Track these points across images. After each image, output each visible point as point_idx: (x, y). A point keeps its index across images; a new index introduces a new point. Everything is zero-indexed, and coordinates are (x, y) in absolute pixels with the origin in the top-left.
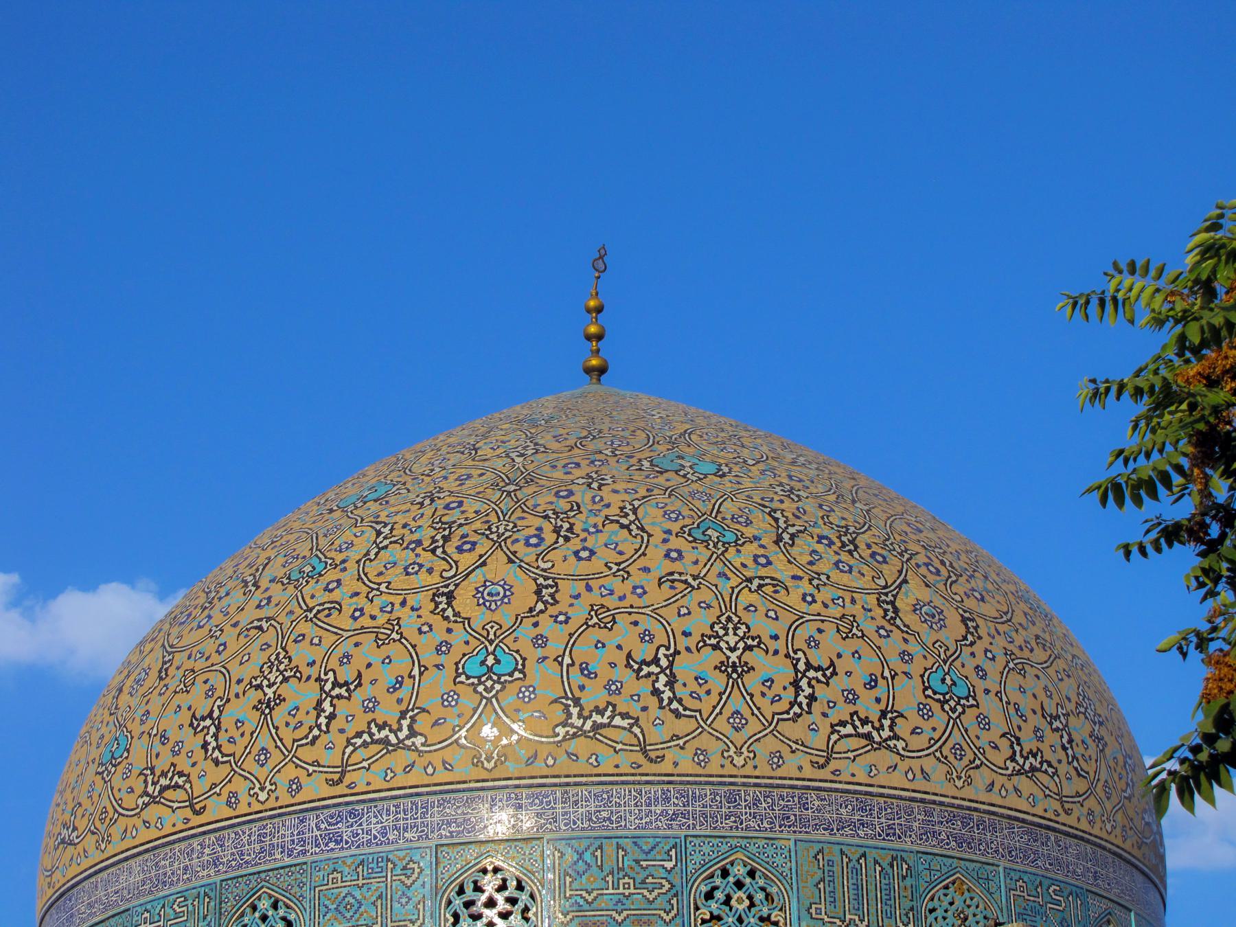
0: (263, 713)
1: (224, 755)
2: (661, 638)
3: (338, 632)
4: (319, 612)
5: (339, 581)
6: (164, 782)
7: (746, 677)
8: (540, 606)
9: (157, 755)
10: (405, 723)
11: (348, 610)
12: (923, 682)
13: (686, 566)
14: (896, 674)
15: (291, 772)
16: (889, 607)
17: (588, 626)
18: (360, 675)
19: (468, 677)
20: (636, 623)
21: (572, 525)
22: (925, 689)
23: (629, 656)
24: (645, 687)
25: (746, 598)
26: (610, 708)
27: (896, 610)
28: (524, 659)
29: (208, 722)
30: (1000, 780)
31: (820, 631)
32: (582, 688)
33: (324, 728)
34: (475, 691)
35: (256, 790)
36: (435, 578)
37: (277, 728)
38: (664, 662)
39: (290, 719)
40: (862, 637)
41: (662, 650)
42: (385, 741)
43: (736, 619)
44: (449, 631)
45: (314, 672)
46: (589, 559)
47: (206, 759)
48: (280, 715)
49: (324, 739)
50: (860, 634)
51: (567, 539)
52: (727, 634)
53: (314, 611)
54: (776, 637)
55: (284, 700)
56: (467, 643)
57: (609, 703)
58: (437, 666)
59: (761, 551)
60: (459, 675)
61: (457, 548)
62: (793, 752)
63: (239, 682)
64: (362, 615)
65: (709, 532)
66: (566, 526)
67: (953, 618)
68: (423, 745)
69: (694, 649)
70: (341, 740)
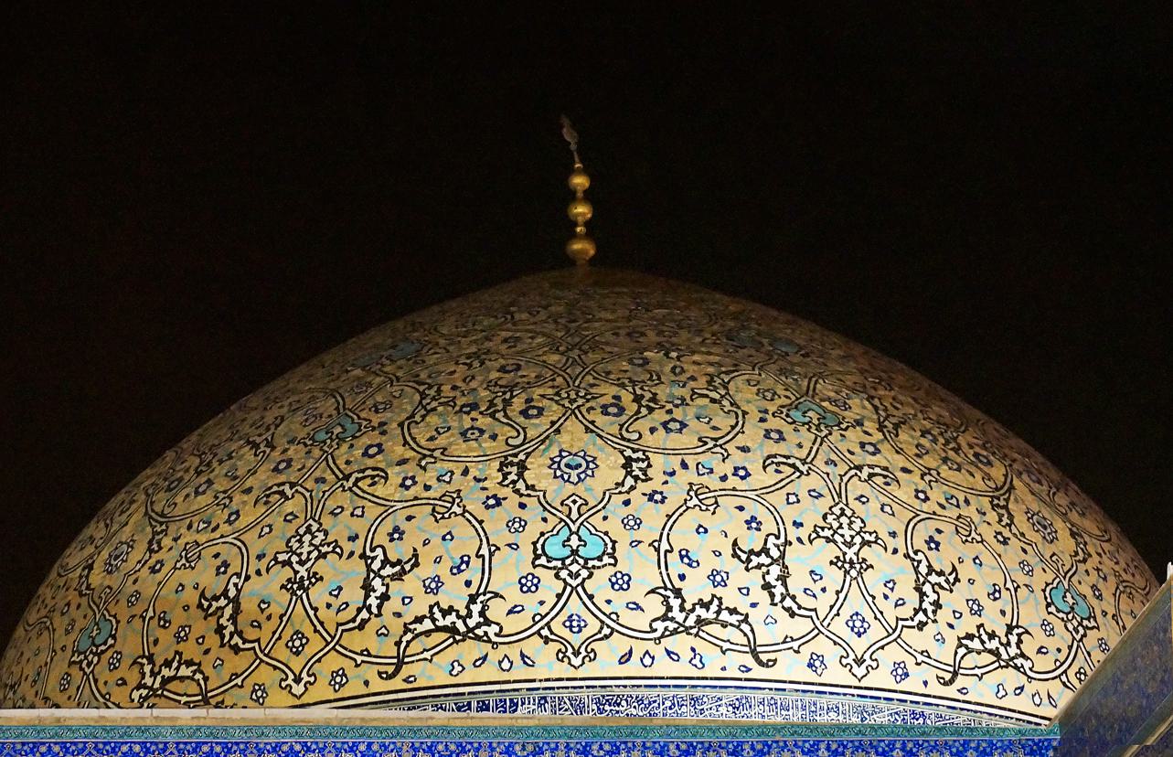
0: (294, 593)
1: (245, 641)
2: (769, 526)
3: (386, 506)
4: (358, 480)
5: (379, 446)
6: (166, 672)
7: (867, 575)
8: (630, 481)
9: (156, 642)
10: (476, 608)
12: (1046, 598)
14: (1018, 586)
16: (1003, 512)
17: (688, 508)
18: (416, 556)
19: (550, 559)
20: (741, 508)
21: (655, 394)
22: (1048, 605)
23: (735, 543)
24: (755, 579)
25: (856, 488)
26: (716, 602)
27: (1011, 517)
28: (614, 542)
29: (223, 602)
31: (939, 531)
32: (682, 577)
33: (375, 610)
34: (557, 576)
35: (290, 681)
36: (499, 446)
37: (316, 610)
38: (775, 553)
39: (331, 600)
40: (982, 542)
41: (772, 539)
42: (452, 630)
43: (848, 513)
47: (222, 645)
48: (319, 594)
49: (375, 623)
50: (979, 539)
51: (651, 410)
52: (840, 527)
53: (352, 479)
54: (893, 534)
55: (321, 579)
56: (545, 520)
57: (714, 596)
58: (509, 545)
59: (867, 439)
60: (537, 557)
61: (521, 413)
62: (918, 664)
63: (260, 557)
64: (415, 483)
65: (810, 414)
68: (496, 635)
69: (805, 540)
70: (396, 627)
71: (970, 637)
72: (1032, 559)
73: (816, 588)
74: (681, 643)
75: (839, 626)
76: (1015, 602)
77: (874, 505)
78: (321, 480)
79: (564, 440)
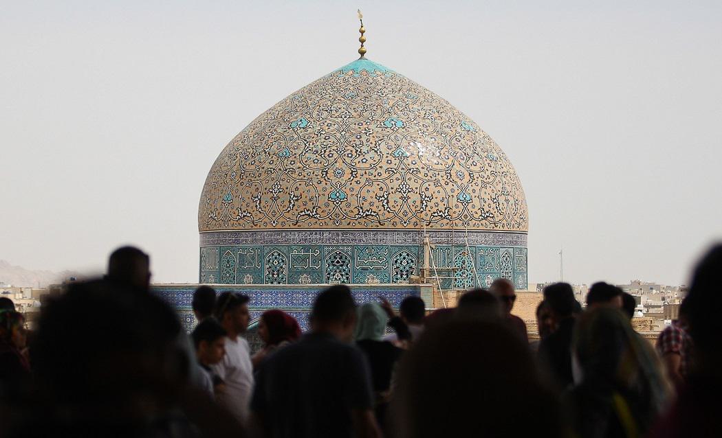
11: (297, 173)
13: (392, 166)
15: (282, 220)
20: (378, 185)
25: (409, 176)
27: (451, 175)
29: (257, 199)
30: (477, 222)
32: (363, 204)
38: (386, 197)
42: (309, 215)
44: (326, 184)
45: (288, 191)
46: (365, 162)
51: (359, 155)
59: (413, 159)
63: (266, 189)
66: (359, 150)
67: (467, 174)
71: (434, 213)
72: (455, 187)
73: (395, 205)
74: (362, 220)
75: (401, 215)
76: (448, 202)
77: (413, 180)
78: (280, 169)
79: (338, 164)
